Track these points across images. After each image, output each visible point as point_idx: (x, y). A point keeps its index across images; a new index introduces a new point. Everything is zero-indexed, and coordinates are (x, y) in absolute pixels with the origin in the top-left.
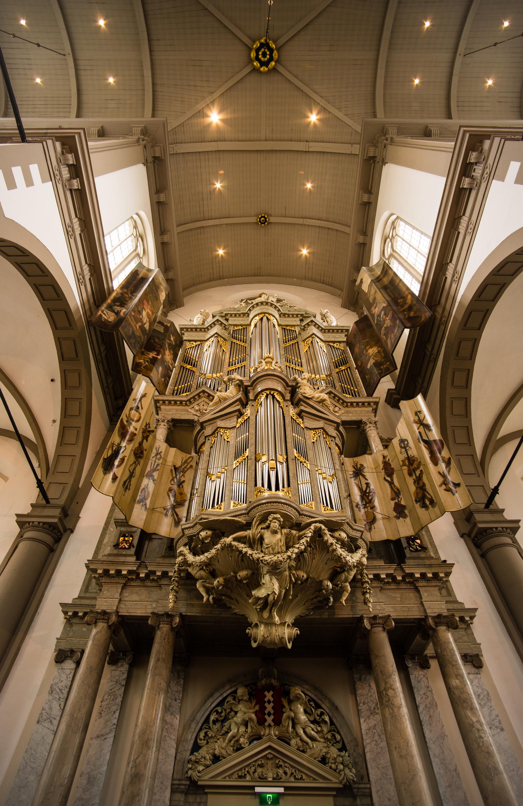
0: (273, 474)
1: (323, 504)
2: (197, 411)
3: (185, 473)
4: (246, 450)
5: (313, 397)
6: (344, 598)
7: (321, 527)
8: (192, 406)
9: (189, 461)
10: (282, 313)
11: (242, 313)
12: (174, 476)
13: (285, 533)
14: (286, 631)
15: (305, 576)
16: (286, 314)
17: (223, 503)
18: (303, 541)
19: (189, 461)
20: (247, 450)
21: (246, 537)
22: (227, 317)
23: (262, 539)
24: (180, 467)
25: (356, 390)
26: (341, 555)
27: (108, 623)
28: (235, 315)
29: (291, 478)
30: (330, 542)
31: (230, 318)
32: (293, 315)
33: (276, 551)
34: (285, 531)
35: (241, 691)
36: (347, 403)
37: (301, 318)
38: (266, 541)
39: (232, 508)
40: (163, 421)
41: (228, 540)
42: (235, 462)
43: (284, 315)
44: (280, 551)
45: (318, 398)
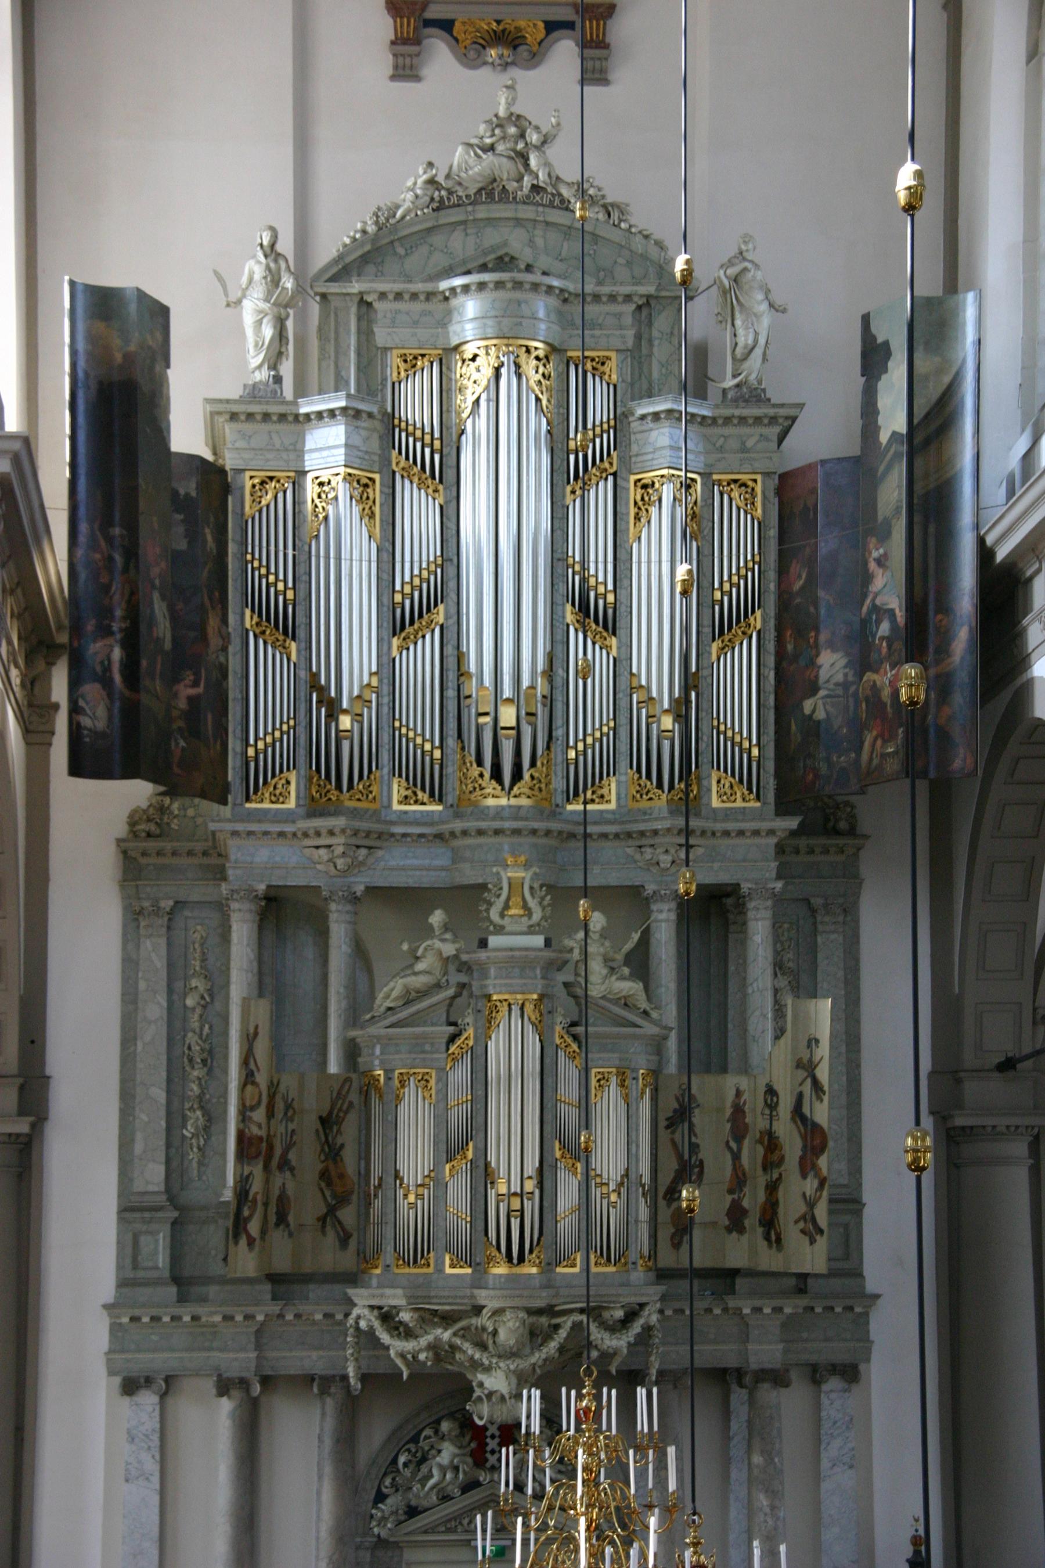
0: (515, 1224)
3: (341, 1123)
4: (467, 1144)
9: (344, 1093)
10: (570, 293)
12: (323, 1139)
17: (432, 1254)
18: (553, 1345)
19: (344, 1093)
20: (471, 1144)
23: (495, 1333)
24: (330, 1113)
25: (755, 752)
28: (399, 296)
29: (545, 1211)
32: (612, 298)
35: (445, 1426)
37: (640, 303)
39: (449, 1271)
41: (447, 1336)
42: (448, 1167)
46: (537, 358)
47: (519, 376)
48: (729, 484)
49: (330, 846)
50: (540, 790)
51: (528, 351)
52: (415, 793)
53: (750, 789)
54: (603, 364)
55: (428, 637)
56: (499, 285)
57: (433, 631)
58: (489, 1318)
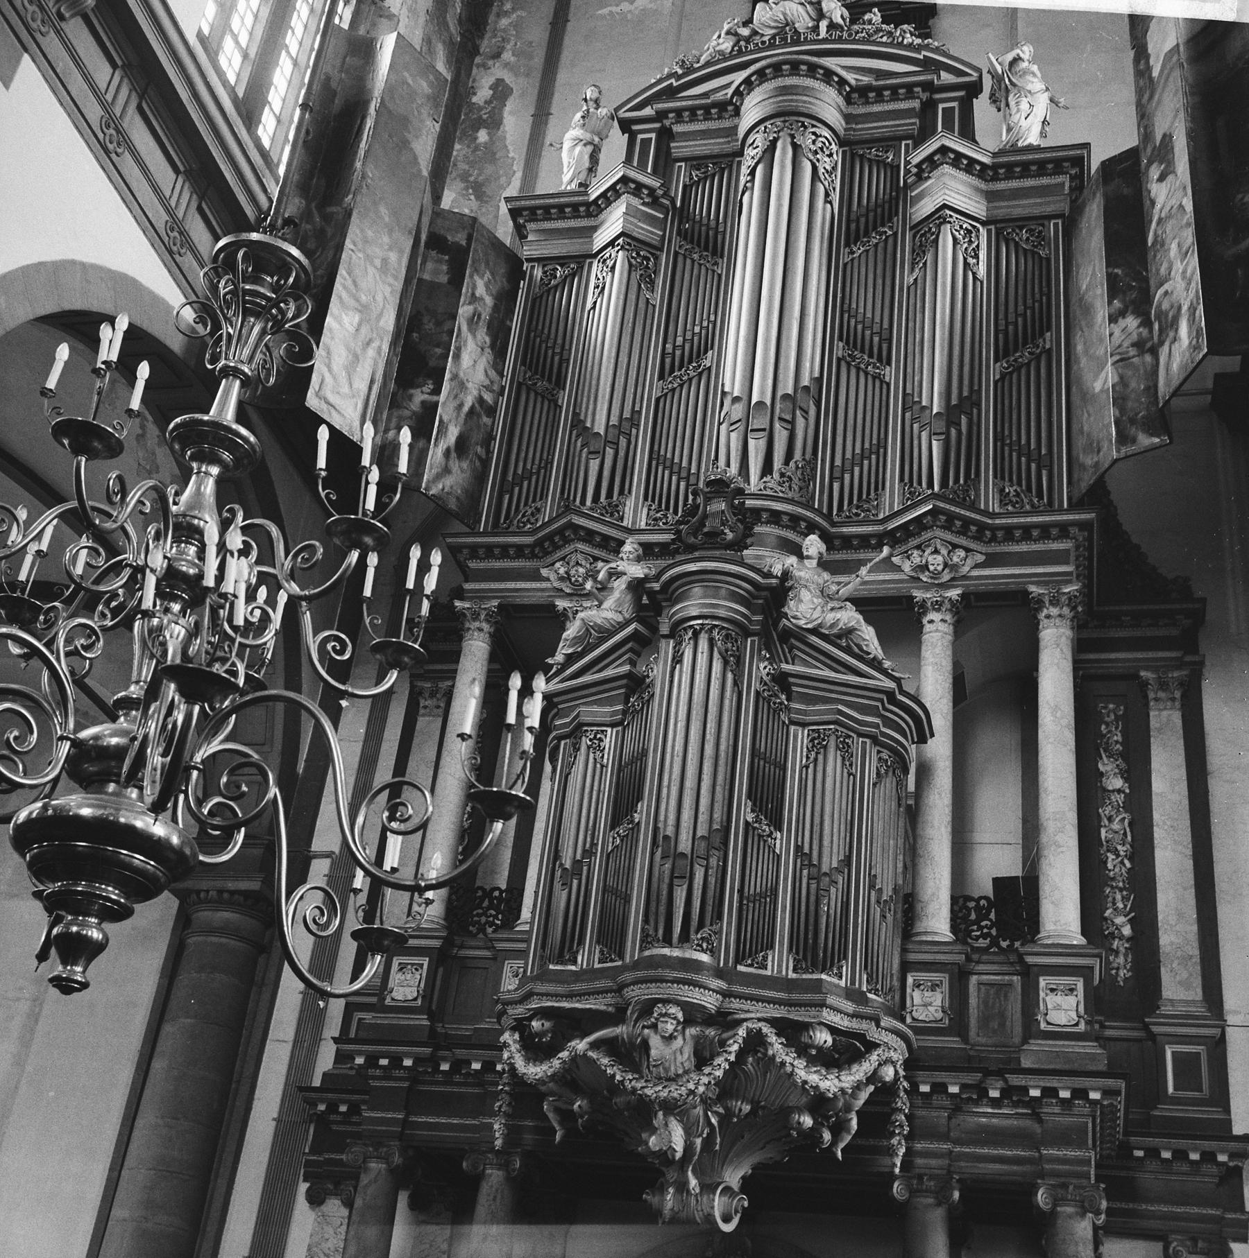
1: (797, 953)
2: (561, 579)
5: (820, 625)
6: (842, 1145)
7: (760, 1029)
8: (549, 560)
10: (853, 90)
11: (714, 105)
13: (692, 1036)
14: (716, 1203)
15: (747, 1108)
16: (869, 88)
21: (616, 1038)
22: (667, 123)
23: (645, 1045)
26: (805, 1082)
27: (387, 1163)
30: (778, 1060)
31: (678, 128)
33: (672, 1074)
34: (692, 1031)
36: (994, 529)
37: (924, 96)
38: (653, 1052)
40: (476, 617)
41: (581, 1045)
43: (863, 91)
44: (680, 1072)
45: (832, 626)
46: (814, 133)
47: (796, 147)
48: (1013, 230)
49: (563, 559)
50: (790, 488)
51: (806, 127)
52: (665, 516)
53: (1040, 495)
54: (887, 152)
55: (694, 382)
56: (777, 68)
57: (700, 374)
58: (636, 1021)
